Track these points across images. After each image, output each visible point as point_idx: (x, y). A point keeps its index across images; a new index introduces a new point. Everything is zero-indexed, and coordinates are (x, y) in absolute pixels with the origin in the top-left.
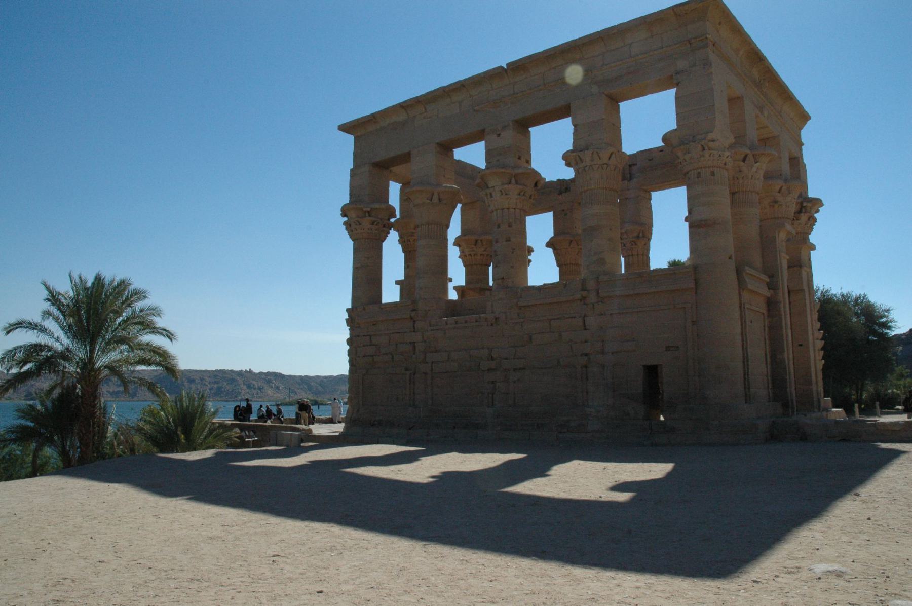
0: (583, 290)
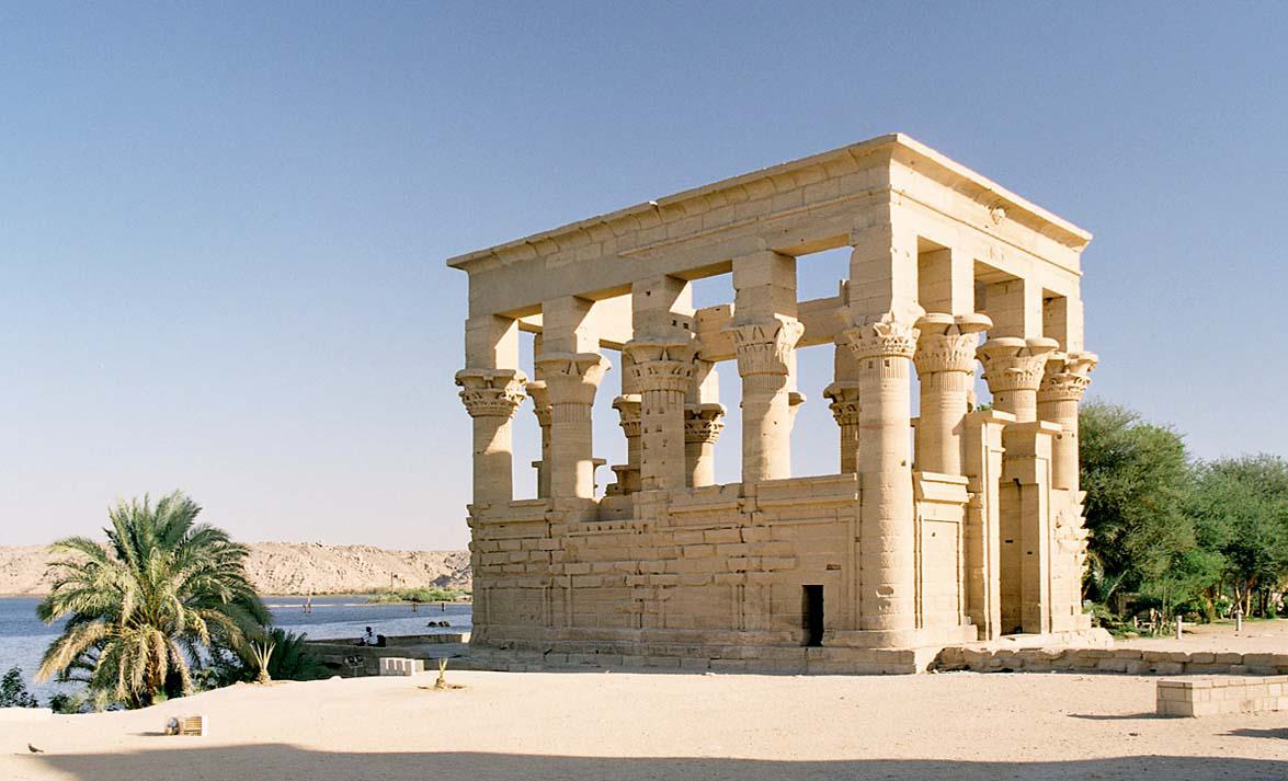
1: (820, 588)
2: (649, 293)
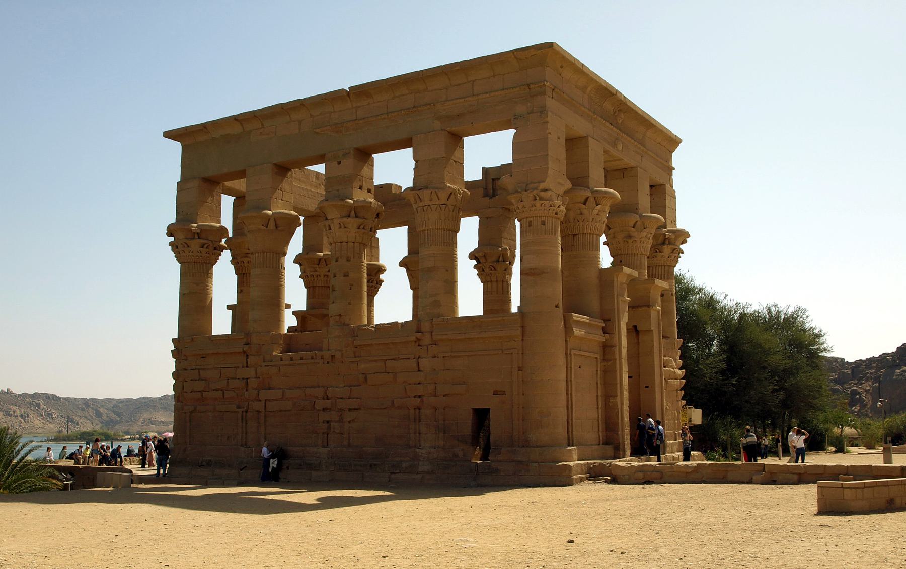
0: (419, 331)
1: (487, 411)
2: (339, 163)
